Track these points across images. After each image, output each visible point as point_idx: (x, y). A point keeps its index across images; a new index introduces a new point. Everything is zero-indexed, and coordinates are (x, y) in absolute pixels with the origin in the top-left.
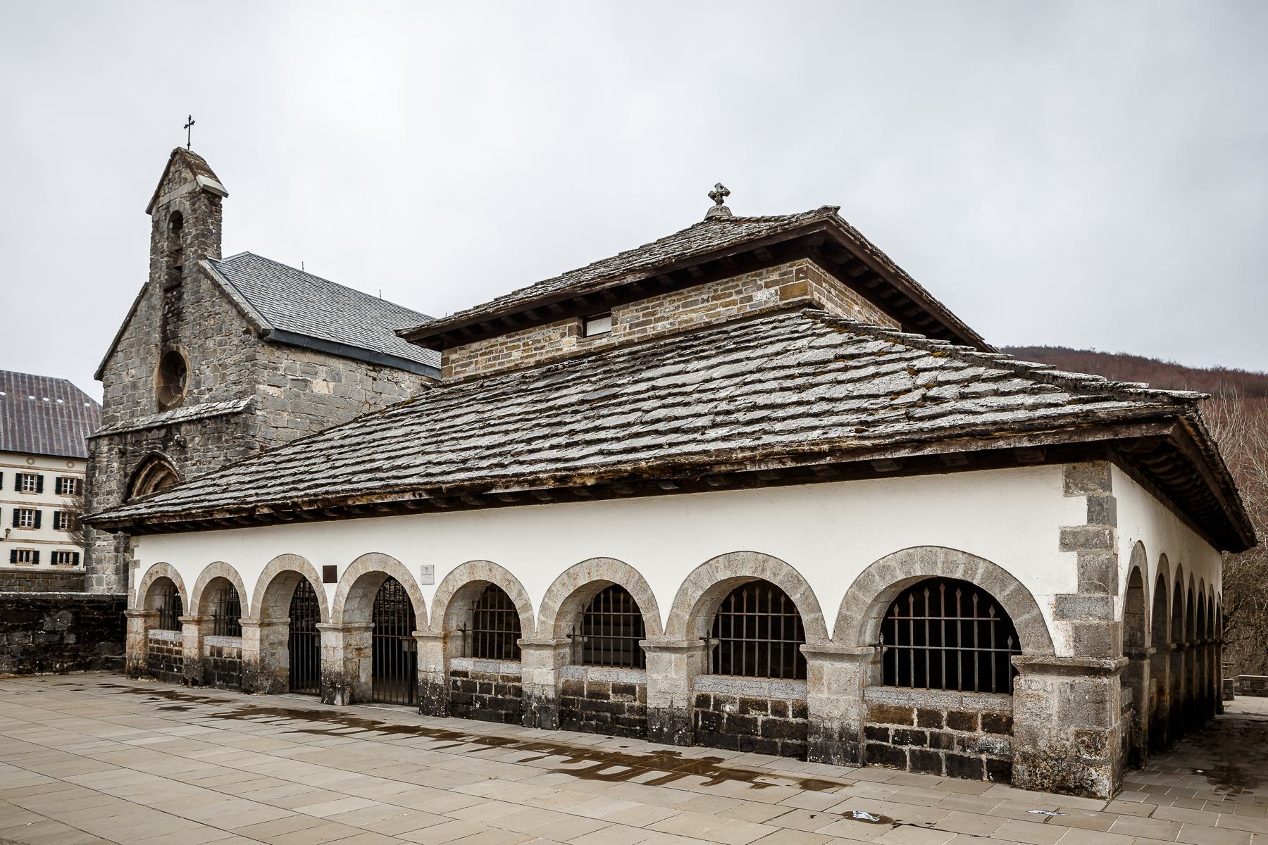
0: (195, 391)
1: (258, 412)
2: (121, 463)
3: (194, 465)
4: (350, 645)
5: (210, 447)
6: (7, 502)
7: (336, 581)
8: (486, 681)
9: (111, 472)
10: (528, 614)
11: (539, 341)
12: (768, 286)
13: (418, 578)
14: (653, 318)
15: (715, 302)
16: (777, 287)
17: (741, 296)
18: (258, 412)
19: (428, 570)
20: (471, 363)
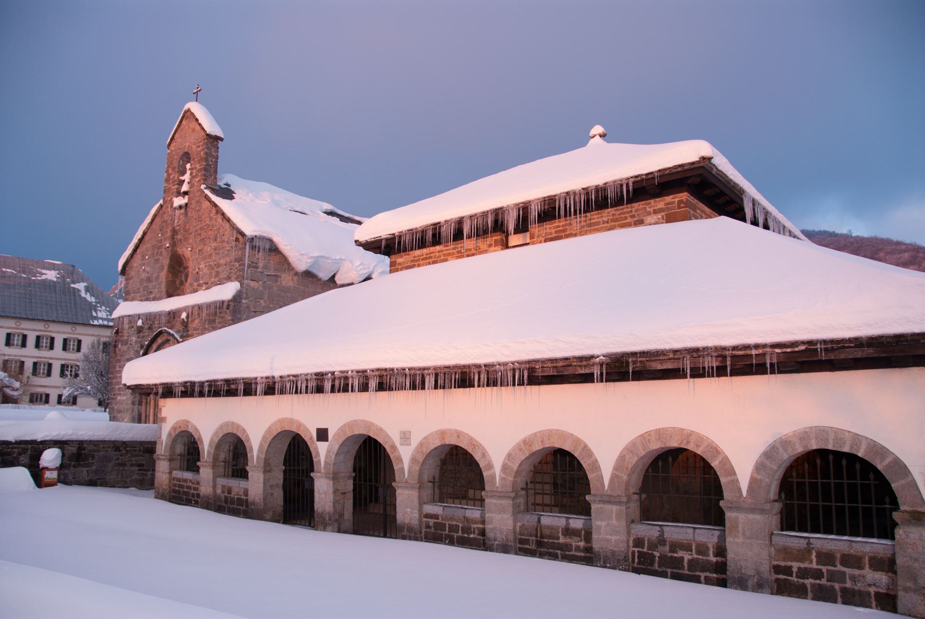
0: (195, 284)
1: (244, 301)
2: (138, 337)
4: (338, 490)
5: (207, 326)
6: (29, 357)
7: (328, 441)
8: (454, 523)
9: (131, 344)
10: (490, 472)
11: (470, 250)
12: (655, 212)
13: (397, 441)
14: (563, 234)
15: (613, 223)
16: (663, 214)
17: (635, 219)
18: (244, 301)
19: (406, 437)
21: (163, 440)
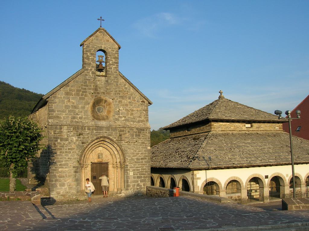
3: (126, 143)
5: (135, 137)
12: (277, 126)
13: (285, 176)
19: (287, 175)
20: (220, 127)
21: (199, 186)
